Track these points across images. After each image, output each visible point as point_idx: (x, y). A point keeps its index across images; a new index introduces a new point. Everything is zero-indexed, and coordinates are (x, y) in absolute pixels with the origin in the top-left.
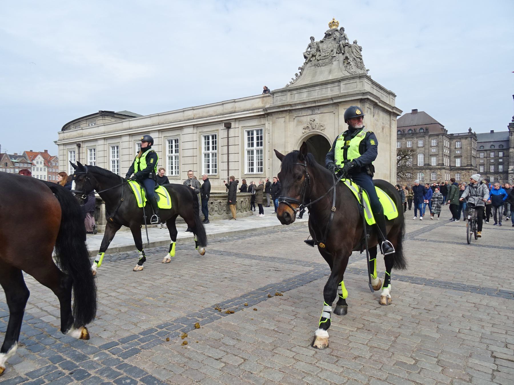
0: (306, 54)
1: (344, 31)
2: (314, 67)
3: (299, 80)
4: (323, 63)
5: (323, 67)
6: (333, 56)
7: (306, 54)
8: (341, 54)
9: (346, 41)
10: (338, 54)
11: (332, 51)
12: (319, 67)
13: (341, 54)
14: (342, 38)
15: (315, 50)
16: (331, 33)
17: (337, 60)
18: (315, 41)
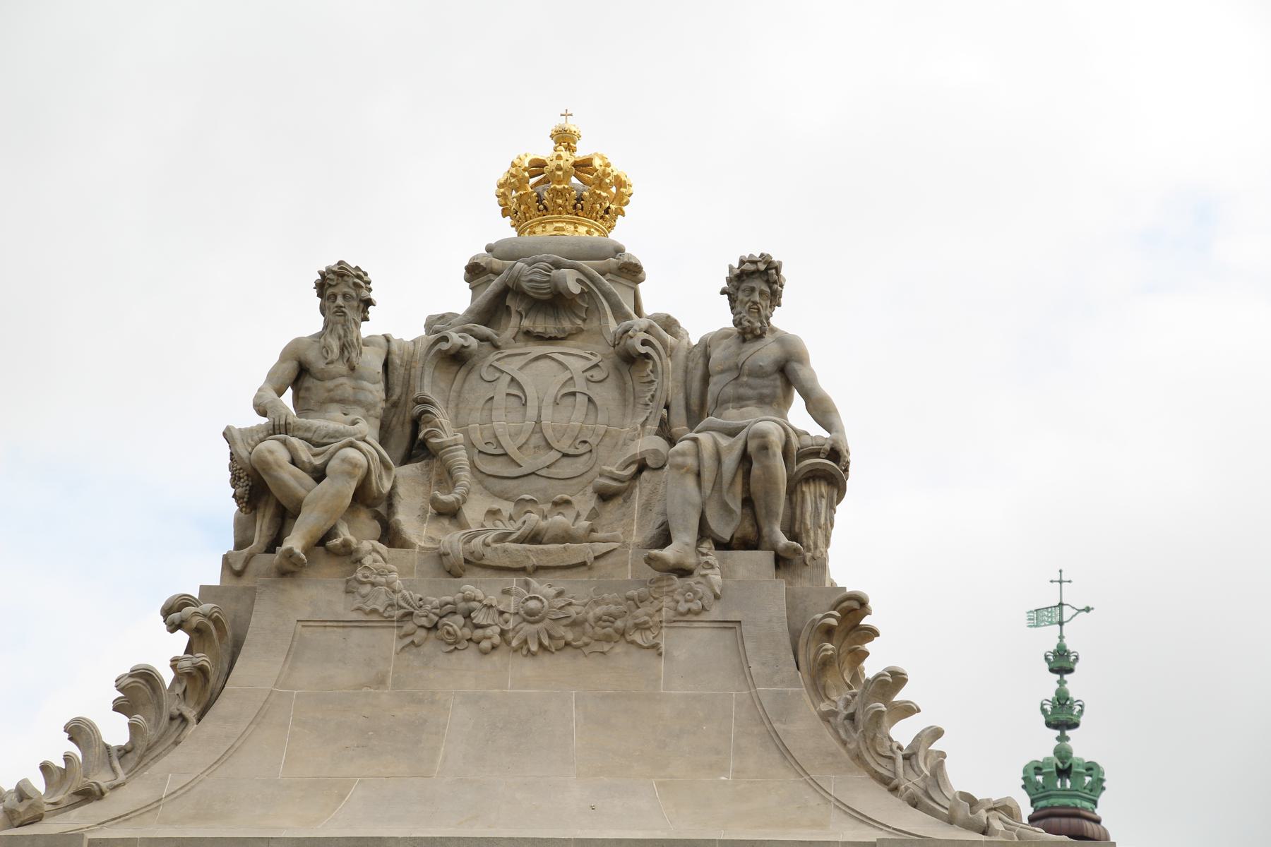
0: (283, 455)
1: (774, 298)
2: (389, 639)
3: (175, 758)
4: (531, 616)
5: (528, 668)
6: (669, 554)
7: (274, 450)
8: (763, 558)
9: (798, 415)
10: (721, 545)
11: (605, 496)
12: (469, 656)
13: (763, 558)
14: (758, 373)
15: (368, 428)
16: (575, 289)
17: (715, 613)
18: (366, 330)
